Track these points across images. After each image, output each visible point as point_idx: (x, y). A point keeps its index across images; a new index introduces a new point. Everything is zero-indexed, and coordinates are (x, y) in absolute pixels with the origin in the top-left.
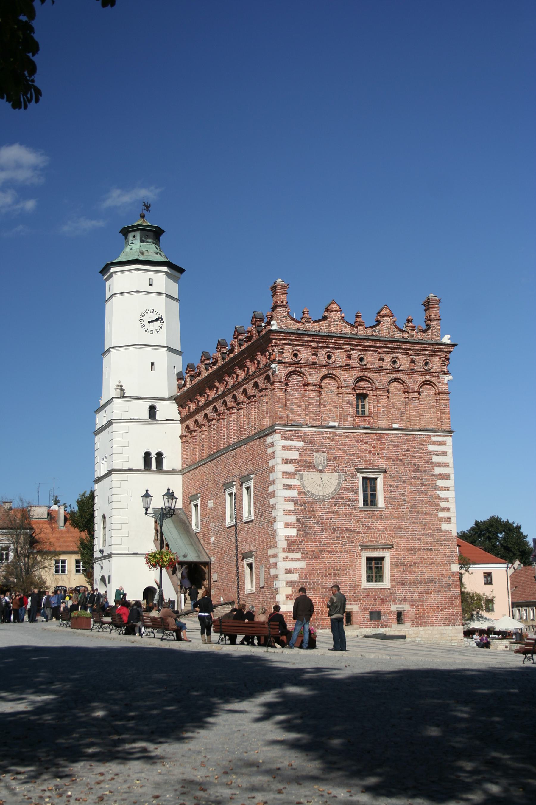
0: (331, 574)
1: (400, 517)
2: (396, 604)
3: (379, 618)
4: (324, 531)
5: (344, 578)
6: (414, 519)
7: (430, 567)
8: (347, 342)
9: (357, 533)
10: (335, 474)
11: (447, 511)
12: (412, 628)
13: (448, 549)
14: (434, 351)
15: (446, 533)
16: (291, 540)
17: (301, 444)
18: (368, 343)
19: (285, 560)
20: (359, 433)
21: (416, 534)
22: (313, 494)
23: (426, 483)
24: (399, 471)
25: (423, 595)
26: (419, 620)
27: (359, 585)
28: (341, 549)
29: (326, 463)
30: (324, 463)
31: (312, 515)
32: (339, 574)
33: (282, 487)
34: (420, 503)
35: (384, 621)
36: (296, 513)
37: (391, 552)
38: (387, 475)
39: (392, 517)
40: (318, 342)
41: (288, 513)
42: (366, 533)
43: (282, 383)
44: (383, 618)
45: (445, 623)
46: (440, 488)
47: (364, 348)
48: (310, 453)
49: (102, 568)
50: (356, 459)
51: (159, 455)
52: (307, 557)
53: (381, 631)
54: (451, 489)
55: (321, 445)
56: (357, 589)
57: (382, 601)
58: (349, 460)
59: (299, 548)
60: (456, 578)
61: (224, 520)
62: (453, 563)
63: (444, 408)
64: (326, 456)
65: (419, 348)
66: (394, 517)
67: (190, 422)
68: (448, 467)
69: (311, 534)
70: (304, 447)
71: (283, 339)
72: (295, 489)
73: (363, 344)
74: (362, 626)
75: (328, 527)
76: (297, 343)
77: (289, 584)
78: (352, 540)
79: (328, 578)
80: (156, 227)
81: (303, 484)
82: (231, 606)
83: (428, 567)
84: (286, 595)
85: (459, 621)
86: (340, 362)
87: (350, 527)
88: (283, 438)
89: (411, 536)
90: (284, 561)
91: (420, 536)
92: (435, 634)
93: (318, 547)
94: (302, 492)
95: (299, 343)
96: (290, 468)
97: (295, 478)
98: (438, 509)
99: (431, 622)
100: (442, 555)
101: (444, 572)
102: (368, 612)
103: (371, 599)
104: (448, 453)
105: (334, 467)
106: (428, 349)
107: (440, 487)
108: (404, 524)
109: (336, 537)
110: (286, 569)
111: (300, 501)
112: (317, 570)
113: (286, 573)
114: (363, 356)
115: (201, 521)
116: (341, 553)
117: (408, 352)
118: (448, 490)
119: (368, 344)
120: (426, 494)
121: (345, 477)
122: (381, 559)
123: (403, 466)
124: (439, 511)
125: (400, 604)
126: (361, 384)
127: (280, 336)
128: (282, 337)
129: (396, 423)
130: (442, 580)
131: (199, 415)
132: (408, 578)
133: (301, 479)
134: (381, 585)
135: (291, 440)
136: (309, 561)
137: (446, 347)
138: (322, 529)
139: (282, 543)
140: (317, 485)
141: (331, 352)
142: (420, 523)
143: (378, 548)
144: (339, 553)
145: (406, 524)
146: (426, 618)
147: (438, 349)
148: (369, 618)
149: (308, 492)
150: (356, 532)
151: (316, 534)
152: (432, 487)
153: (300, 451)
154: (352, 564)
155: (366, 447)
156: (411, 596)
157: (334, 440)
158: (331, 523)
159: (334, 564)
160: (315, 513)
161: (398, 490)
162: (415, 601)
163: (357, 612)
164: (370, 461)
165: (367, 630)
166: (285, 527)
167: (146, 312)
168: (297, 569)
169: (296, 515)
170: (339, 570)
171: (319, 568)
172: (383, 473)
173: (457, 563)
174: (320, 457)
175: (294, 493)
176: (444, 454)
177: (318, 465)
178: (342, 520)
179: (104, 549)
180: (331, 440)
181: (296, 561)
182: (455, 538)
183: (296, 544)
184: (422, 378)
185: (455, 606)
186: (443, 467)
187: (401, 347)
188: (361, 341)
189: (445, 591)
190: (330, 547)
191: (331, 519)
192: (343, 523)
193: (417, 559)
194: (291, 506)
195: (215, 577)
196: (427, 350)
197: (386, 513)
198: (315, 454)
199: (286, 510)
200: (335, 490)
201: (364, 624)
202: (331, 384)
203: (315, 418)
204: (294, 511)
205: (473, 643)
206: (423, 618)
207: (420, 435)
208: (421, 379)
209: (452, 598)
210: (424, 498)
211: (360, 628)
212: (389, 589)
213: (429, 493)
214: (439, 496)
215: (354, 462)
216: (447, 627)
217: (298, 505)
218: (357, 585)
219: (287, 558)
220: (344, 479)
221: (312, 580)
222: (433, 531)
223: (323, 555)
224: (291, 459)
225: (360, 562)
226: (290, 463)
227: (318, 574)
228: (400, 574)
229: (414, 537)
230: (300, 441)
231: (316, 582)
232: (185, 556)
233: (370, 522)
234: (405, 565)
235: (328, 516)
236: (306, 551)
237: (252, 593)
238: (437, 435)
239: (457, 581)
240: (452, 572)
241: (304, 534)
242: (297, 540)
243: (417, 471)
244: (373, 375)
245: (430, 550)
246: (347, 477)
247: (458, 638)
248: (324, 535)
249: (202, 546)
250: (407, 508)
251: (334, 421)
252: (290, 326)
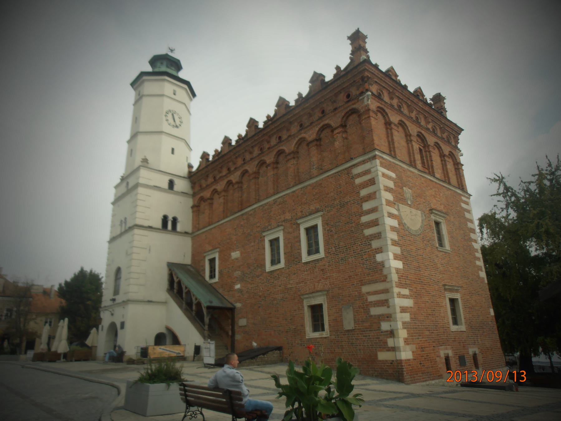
16: (400, 274)
17: (393, 175)
41: (395, 243)
44: (468, 364)
49: (112, 314)
51: (175, 221)
57: (464, 345)
61: (264, 265)
64: (411, 192)
67: (207, 194)
80: (179, 61)
82: (279, 352)
113: (401, 312)
115: (219, 272)
131: (219, 184)
133: (399, 210)
139: (394, 277)
141: (401, 103)
167: (170, 111)
174: (408, 192)
179: (117, 297)
192: (430, 261)
195: (242, 322)
198: (404, 188)
212: (465, 331)
219: (400, 293)
226: (389, 192)
227: (422, 314)
232: (211, 302)
237: (321, 338)
249: (220, 294)
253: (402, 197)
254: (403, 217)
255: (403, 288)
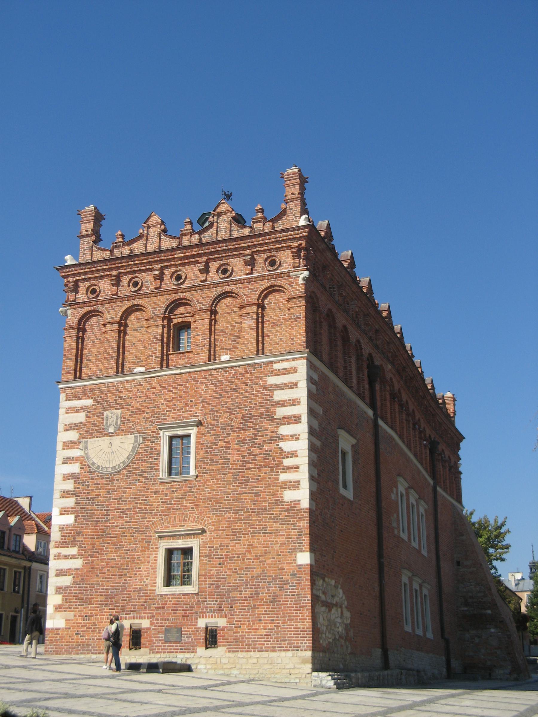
0: (116, 575)
1: (219, 487)
2: (206, 617)
3: (179, 640)
4: (109, 515)
5: (132, 580)
6: (241, 488)
7: (262, 559)
8: (155, 259)
9: (154, 515)
10: (129, 436)
11: (294, 472)
12: (228, 654)
13: (292, 529)
14: (280, 242)
15: (291, 504)
17: (88, 402)
18: (182, 253)
19: (57, 557)
20: (166, 375)
21: (241, 510)
22: (99, 466)
23: (263, 433)
24: (221, 420)
25: (250, 603)
26: (240, 642)
27: (152, 590)
28: (131, 539)
29: (119, 423)
30: (117, 422)
31: (96, 495)
32: (126, 575)
33: (61, 462)
34: (250, 463)
35: (185, 643)
36: (75, 494)
37: (202, 539)
38: (203, 429)
39: (206, 488)
40: (118, 268)
41: (66, 494)
42: (166, 515)
43: (73, 329)
44: (184, 639)
45: (283, 647)
46: (281, 438)
47: (179, 262)
48: (100, 413)
50: (160, 412)
52: (85, 552)
53: (179, 658)
54: (301, 437)
55: (115, 400)
56: (149, 596)
57: (186, 613)
58: (149, 415)
59: (75, 541)
60: (305, 574)
62: (301, 551)
63: (295, 319)
64: (119, 414)
65: (256, 243)
66: (209, 488)
68: (299, 404)
69: (92, 521)
70: (93, 405)
71: (75, 275)
72: (77, 463)
73: (175, 256)
74: (152, 651)
75: (115, 509)
76: (93, 276)
77: (59, 590)
78: (147, 526)
79: (111, 581)
81: (87, 454)
83: (259, 559)
84: (55, 606)
85: (305, 643)
86: (149, 287)
87: (145, 508)
88: (69, 398)
89: (233, 513)
90: (55, 559)
91: (249, 512)
92: (264, 664)
93: (101, 538)
94: (85, 465)
95: (96, 275)
96: (73, 435)
97: (78, 448)
98: (280, 469)
99: (259, 644)
100: (283, 539)
101: (285, 566)
102: (163, 630)
103: (168, 610)
104: (299, 384)
105: (130, 427)
106: (270, 241)
107: (284, 436)
108: (224, 497)
109: (126, 522)
110: (57, 570)
111: (82, 478)
112: (97, 570)
113: (57, 575)
114: (180, 273)
116: (130, 545)
117: (242, 252)
118: (297, 439)
119: (182, 255)
120: (260, 449)
121: (143, 438)
122: (187, 552)
123: (227, 412)
124: (281, 472)
125: (212, 617)
126: (182, 310)
127: (69, 271)
128: (72, 273)
129: (227, 354)
130: (282, 578)
132: (225, 578)
133: (86, 448)
134: (183, 590)
135: (78, 399)
136: (86, 558)
137: (296, 232)
138: (107, 513)
140: (105, 453)
142: (249, 493)
143: (180, 535)
144: (127, 545)
145: (227, 497)
146: (251, 638)
147: (284, 238)
148: (164, 638)
149: (93, 464)
150: (153, 514)
151: (99, 521)
152: (271, 437)
153: (88, 412)
154: (145, 560)
155: (175, 393)
156: (230, 604)
157: (132, 391)
158: (120, 504)
159: (120, 561)
160: (101, 492)
161: (218, 448)
162: (236, 612)
163: (149, 629)
164: (180, 412)
165: (158, 655)
166: (61, 514)
168: (70, 569)
169: (76, 496)
170: (126, 569)
171: (99, 568)
172: (197, 426)
173: (307, 551)
175: (75, 468)
176: (294, 385)
177: (108, 427)
178: (135, 498)
180: (128, 391)
181: (71, 558)
182: (305, 512)
183: (72, 536)
184: (266, 284)
185: (300, 619)
186: (290, 406)
187: (230, 247)
188: (173, 253)
189: (285, 595)
190: (116, 537)
191: (120, 499)
193: (240, 548)
194: (70, 485)
196: (269, 243)
197: (198, 484)
199: (64, 492)
200: (128, 458)
201: (156, 647)
202: (140, 319)
203: (110, 366)
204: (73, 491)
205: (328, 681)
206: (246, 638)
207: (255, 364)
208: (261, 285)
209: (297, 607)
210: (257, 455)
211: (150, 653)
212: (197, 594)
213: (266, 447)
214: (282, 450)
215: (157, 417)
216: (283, 654)
217: (79, 483)
218: (150, 590)
219: (59, 554)
220: (141, 441)
221: (89, 584)
222: (269, 503)
223: (106, 548)
224: (75, 424)
225: (156, 557)
226: (74, 429)
227: (97, 576)
228: (214, 572)
229: (239, 515)
230: (89, 399)
231: (94, 587)
233: (173, 498)
234: (223, 558)
235: (117, 494)
236: (84, 544)
238: (283, 361)
239: (306, 580)
240: (298, 565)
241: (83, 522)
242: (73, 530)
243: (248, 417)
244: (191, 295)
245: (263, 533)
246: (146, 438)
247: (301, 671)
248: (109, 520)
250: (229, 473)
251: (141, 366)
252: (96, 257)
253: (97, 428)
254: (92, 456)
255: (68, 547)
